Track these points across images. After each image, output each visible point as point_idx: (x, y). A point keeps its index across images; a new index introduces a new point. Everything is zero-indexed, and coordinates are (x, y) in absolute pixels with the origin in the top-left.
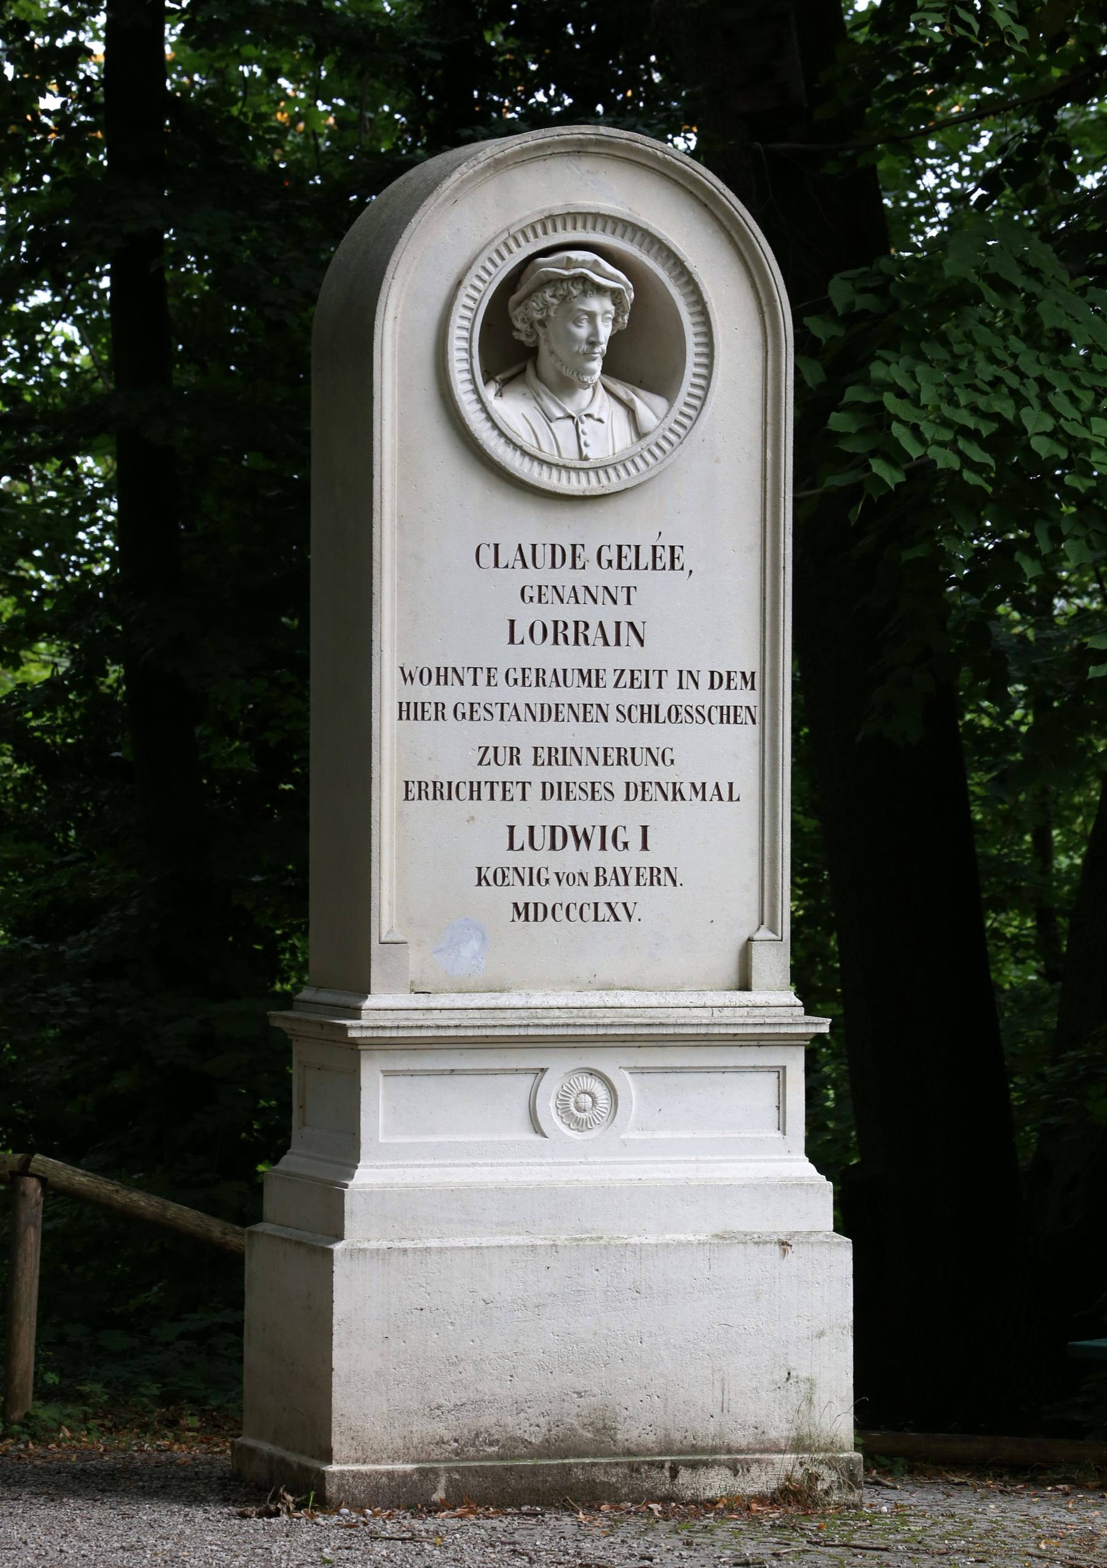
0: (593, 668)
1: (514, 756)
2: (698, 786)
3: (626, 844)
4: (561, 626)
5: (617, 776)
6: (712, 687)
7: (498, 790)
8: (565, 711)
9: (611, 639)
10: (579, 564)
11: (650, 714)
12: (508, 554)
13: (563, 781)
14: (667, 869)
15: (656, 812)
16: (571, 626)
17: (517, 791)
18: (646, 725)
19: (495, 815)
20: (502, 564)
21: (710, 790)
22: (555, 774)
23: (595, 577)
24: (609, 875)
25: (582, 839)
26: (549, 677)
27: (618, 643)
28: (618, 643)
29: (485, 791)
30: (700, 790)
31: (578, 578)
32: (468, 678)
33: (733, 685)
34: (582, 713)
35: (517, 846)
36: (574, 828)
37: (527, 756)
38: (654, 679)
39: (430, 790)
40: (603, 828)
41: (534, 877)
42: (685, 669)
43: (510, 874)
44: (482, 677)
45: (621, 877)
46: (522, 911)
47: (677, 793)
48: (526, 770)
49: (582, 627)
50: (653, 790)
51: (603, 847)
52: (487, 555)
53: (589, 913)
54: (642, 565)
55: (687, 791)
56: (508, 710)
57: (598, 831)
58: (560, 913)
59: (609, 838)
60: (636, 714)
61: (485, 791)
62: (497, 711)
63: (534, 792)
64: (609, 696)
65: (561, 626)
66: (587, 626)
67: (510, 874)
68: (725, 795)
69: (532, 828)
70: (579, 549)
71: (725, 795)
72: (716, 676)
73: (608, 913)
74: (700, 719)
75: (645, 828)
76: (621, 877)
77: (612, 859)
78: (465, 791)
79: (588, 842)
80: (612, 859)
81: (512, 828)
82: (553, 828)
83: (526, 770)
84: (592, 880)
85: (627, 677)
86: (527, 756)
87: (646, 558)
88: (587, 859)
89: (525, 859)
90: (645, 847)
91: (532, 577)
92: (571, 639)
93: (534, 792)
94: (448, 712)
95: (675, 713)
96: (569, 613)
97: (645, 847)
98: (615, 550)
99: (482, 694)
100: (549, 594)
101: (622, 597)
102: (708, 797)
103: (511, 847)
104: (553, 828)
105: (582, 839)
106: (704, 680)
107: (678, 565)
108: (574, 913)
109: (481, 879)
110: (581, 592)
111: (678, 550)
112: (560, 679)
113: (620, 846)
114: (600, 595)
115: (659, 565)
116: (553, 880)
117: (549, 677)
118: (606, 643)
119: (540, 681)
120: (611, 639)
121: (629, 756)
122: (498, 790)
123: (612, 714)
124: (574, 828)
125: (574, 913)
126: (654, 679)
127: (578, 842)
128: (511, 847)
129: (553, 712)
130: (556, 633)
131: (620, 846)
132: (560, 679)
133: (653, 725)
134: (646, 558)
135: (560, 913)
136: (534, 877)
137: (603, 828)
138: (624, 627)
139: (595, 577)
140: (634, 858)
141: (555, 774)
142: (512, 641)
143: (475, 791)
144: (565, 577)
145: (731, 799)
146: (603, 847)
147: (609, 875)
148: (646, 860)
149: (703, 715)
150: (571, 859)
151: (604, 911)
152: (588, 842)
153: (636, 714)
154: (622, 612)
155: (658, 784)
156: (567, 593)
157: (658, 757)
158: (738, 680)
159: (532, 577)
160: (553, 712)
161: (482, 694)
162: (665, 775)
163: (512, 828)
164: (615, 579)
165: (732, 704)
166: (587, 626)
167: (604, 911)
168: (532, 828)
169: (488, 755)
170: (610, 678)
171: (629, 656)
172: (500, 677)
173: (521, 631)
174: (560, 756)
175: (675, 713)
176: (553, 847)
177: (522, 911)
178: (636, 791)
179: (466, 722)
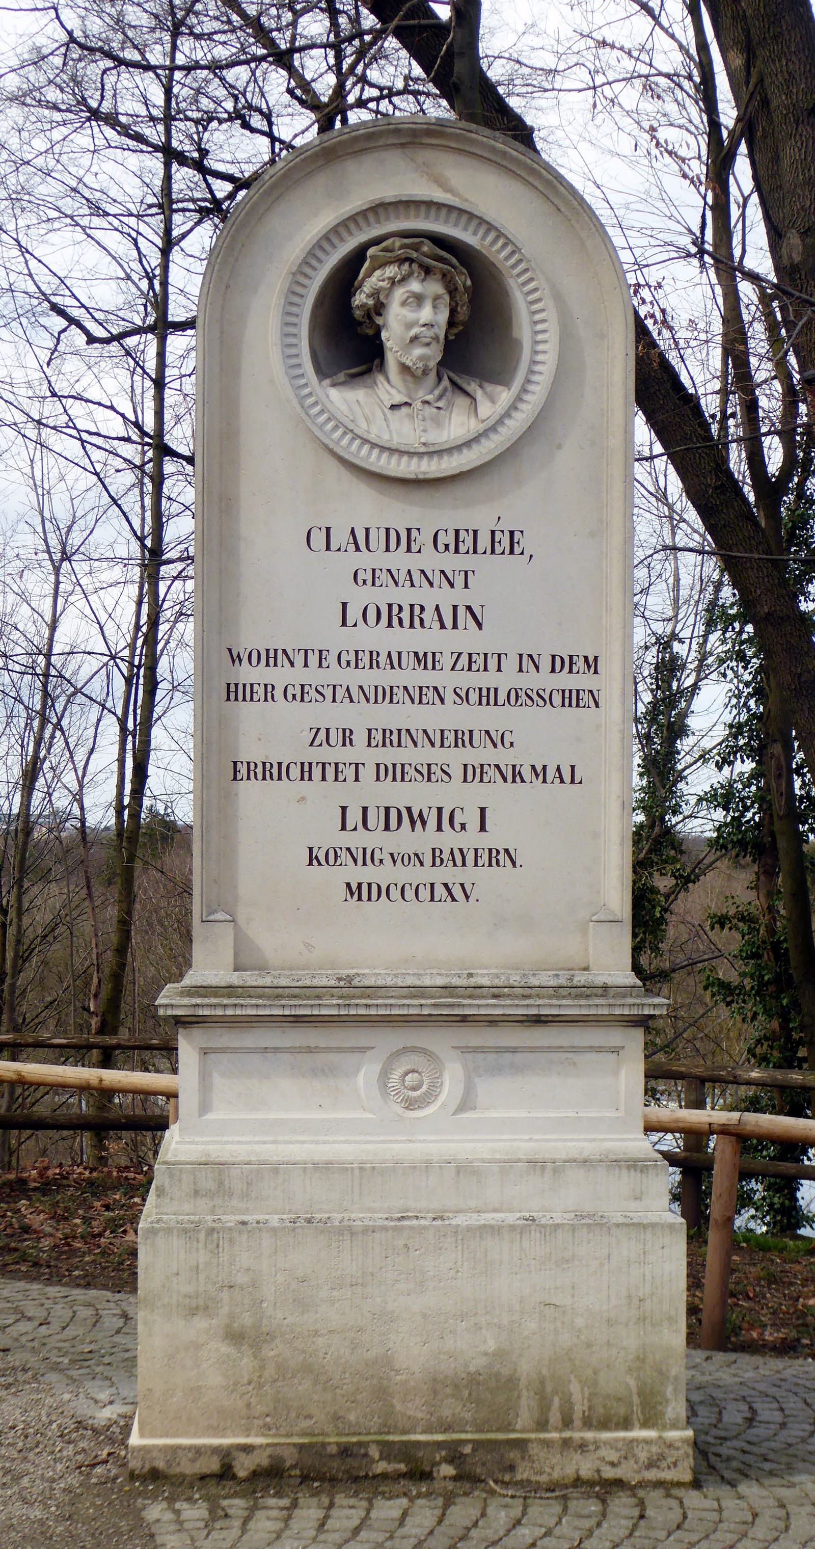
0: (429, 650)
1: (347, 737)
2: (539, 769)
3: (463, 827)
4: (395, 610)
5: (455, 758)
6: (553, 671)
7: (330, 771)
8: (400, 694)
9: (448, 622)
10: (415, 548)
11: (488, 697)
12: (340, 537)
13: (398, 762)
14: (507, 851)
15: (494, 794)
16: (406, 609)
17: (350, 772)
18: (484, 707)
19: (324, 797)
20: (334, 546)
21: (551, 772)
22: (390, 755)
23: (431, 560)
24: (446, 856)
25: (417, 820)
26: (383, 659)
27: (455, 626)
28: (455, 626)
29: (317, 772)
30: (540, 773)
31: (414, 562)
32: (299, 660)
33: (575, 669)
34: (417, 696)
35: (350, 826)
36: (409, 810)
37: (360, 738)
38: (492, 663)
39: (260, 770)
40: (440, 810)
41: (368, 857)
42: (525, 653)
43: (343, 854)
44: (313, 659)
45: (459, 858)
46: (355, 891)
47: (517, 775)
48: (359, 752)
49: (417, 610)
50: (492, 772)
51: (439, 828)
52: (319, 539)
53: (425, 894)
54: (480, 549)
55: (527, 773)
56: (340, 692)
57: (434, 812)
58: (395, 893)
59: (446, 819)
60: (473, 697)
61: (317, 772)
62: (328, 693)
63: (368, 773)
64: (445, 679)
65: (395, 610)
66: (422, 609)
67: (343, 854)
68: (567, 777)
69: (365, 810)
70: (414, 533)
71: (567, 777)
72: (558, 660)
73: (445, 893)
74: (541, 703)
75: (483, 810)
76: (459, 858)
77: (449, 840)
78: (295, 772)
79: (424, 823)
80: (449, 840)
81: (344, 809)
82: (387, 810)
83: (359, 752)
84: (428, 860)
85: (464, 660)
86: (360, 738)
87: (484, 542)
88: (424, 840)
89: (358, 840)
90: (483, 828)
91: (365, 561)
92: (406, 622)
93: (368, 773)
94: (279, 693)
95: (515, 697)
96: (404, 596)
97: (483, 828)
98: (452, 534)
99: (313, 676)
100: (384, 577)
101: (459, 581)
102: (549, 778)
103: (344, 828)
104: (387, 810)
105: (417, 820)
106: (545, 664)
107: (517, 550)
108: (410, 893)
109: (312, 859)
110: (416, 576)
111: (517, 536)
112: (394, 661)
113: (458, 827)
114: (437, 579)
115: (498, 549)
116: (388, 860)
117: (383, 659)
118: (443, 626)
119: (374, 662)
120: (448, 622)
121: (467, 738)
122: (330, 771)
123: (449, 696)
124: (409, 810)
125: (410, 893)
126: (492, 663)
127: (413, 823)
128: (344, 828)
129: (388, 694)
130: (391, 616)
131: (458, 827)
132: (394, 661)
133: (492, 708)
134: (484, 542)
135: (395, 893)
136: (368, 857)
137: (440, 810)
138: (461, 611)
139: (431, 560)
140: (471, 839)
141: (390, 755)
142: (344, 624)
143: (306, 772)
144: (399, 560)
145: (573, 781)
146: (439, 828)
147: (446, 856)
148: (485, 841)
149: (543, 698)
150: (405, 839)
151: (440, 891)
152: (424, 823)
153: (473, 697)
154: (459, 596)
155: (497, 766)
156: (402, 577)
157: (496, 740)
158: (581, 663)
159: (365, 561)
160: (388, 694)
161: (313, 676)
162: (504, 757)
163: (344, 809)
164: (452, 563)
165: (574, 688)
166: (422, 609)
167: (440, 891)
168: (365, 810)
169: (320, 736)
170: (446, 661)
171: (467, 639)
172: (332, 659)
173: (354, 614)
174: (395, 738)
175: (515, 697)
176: (387, 828)
177: (355, 891)
178: (474, 773)
179: (297, 703)
